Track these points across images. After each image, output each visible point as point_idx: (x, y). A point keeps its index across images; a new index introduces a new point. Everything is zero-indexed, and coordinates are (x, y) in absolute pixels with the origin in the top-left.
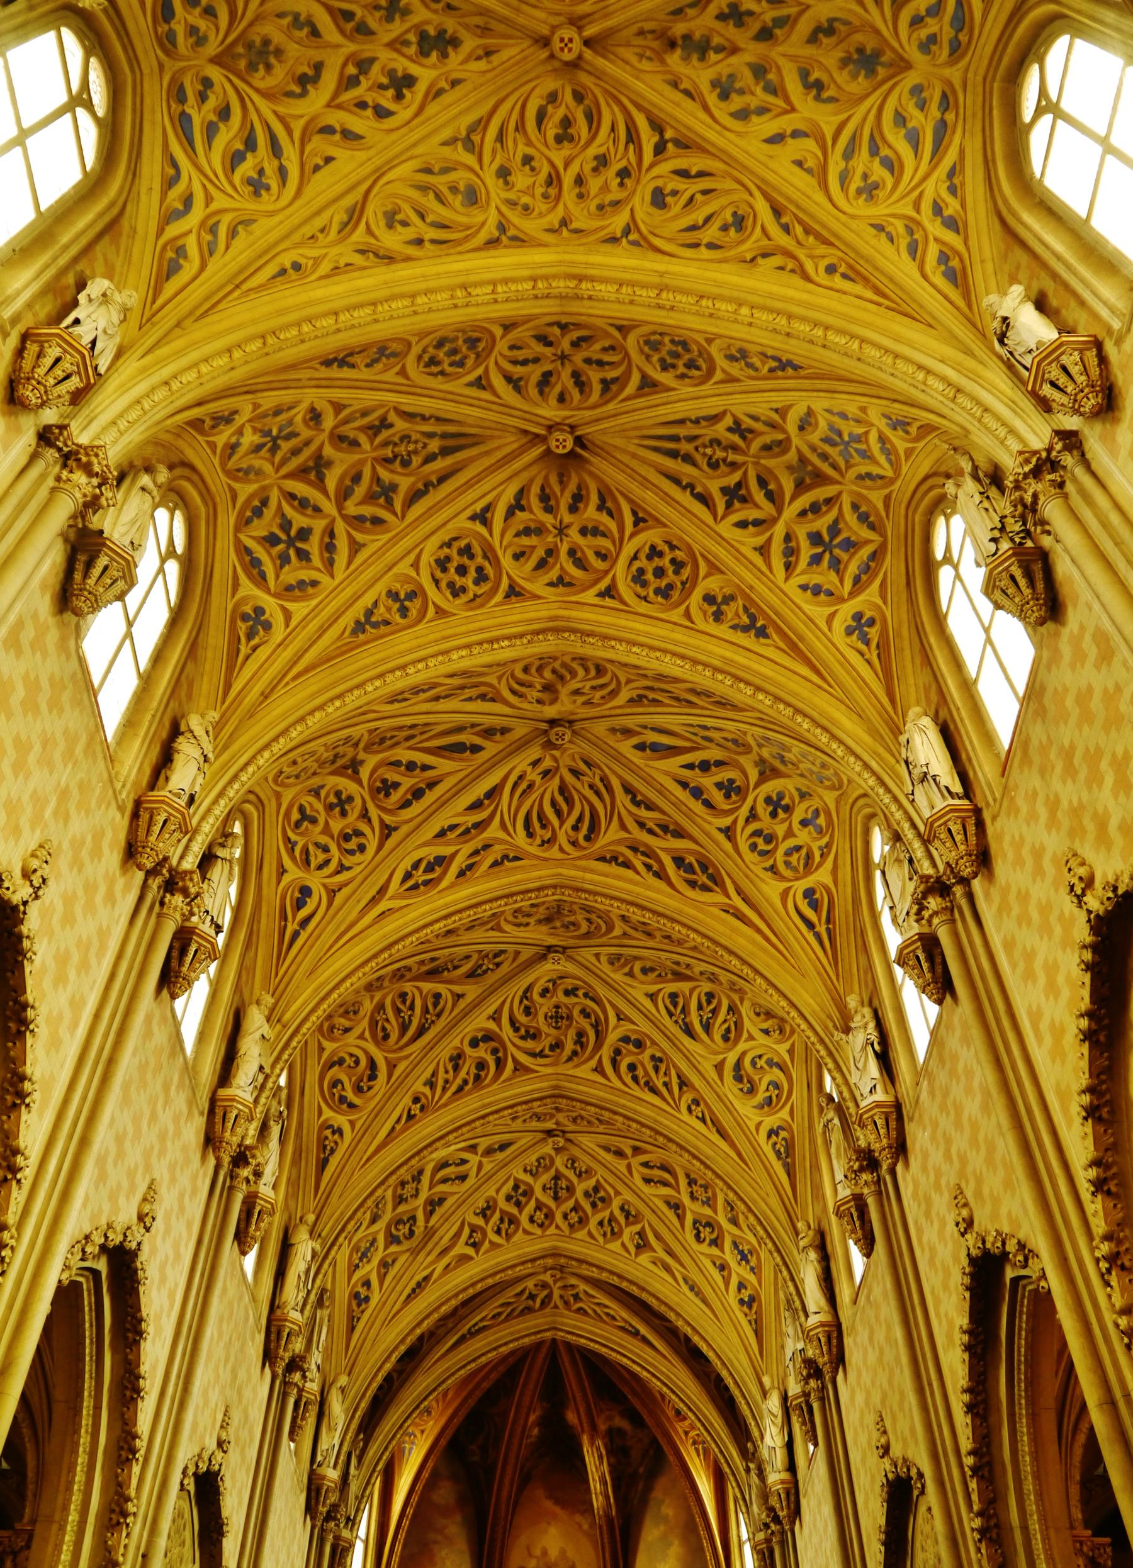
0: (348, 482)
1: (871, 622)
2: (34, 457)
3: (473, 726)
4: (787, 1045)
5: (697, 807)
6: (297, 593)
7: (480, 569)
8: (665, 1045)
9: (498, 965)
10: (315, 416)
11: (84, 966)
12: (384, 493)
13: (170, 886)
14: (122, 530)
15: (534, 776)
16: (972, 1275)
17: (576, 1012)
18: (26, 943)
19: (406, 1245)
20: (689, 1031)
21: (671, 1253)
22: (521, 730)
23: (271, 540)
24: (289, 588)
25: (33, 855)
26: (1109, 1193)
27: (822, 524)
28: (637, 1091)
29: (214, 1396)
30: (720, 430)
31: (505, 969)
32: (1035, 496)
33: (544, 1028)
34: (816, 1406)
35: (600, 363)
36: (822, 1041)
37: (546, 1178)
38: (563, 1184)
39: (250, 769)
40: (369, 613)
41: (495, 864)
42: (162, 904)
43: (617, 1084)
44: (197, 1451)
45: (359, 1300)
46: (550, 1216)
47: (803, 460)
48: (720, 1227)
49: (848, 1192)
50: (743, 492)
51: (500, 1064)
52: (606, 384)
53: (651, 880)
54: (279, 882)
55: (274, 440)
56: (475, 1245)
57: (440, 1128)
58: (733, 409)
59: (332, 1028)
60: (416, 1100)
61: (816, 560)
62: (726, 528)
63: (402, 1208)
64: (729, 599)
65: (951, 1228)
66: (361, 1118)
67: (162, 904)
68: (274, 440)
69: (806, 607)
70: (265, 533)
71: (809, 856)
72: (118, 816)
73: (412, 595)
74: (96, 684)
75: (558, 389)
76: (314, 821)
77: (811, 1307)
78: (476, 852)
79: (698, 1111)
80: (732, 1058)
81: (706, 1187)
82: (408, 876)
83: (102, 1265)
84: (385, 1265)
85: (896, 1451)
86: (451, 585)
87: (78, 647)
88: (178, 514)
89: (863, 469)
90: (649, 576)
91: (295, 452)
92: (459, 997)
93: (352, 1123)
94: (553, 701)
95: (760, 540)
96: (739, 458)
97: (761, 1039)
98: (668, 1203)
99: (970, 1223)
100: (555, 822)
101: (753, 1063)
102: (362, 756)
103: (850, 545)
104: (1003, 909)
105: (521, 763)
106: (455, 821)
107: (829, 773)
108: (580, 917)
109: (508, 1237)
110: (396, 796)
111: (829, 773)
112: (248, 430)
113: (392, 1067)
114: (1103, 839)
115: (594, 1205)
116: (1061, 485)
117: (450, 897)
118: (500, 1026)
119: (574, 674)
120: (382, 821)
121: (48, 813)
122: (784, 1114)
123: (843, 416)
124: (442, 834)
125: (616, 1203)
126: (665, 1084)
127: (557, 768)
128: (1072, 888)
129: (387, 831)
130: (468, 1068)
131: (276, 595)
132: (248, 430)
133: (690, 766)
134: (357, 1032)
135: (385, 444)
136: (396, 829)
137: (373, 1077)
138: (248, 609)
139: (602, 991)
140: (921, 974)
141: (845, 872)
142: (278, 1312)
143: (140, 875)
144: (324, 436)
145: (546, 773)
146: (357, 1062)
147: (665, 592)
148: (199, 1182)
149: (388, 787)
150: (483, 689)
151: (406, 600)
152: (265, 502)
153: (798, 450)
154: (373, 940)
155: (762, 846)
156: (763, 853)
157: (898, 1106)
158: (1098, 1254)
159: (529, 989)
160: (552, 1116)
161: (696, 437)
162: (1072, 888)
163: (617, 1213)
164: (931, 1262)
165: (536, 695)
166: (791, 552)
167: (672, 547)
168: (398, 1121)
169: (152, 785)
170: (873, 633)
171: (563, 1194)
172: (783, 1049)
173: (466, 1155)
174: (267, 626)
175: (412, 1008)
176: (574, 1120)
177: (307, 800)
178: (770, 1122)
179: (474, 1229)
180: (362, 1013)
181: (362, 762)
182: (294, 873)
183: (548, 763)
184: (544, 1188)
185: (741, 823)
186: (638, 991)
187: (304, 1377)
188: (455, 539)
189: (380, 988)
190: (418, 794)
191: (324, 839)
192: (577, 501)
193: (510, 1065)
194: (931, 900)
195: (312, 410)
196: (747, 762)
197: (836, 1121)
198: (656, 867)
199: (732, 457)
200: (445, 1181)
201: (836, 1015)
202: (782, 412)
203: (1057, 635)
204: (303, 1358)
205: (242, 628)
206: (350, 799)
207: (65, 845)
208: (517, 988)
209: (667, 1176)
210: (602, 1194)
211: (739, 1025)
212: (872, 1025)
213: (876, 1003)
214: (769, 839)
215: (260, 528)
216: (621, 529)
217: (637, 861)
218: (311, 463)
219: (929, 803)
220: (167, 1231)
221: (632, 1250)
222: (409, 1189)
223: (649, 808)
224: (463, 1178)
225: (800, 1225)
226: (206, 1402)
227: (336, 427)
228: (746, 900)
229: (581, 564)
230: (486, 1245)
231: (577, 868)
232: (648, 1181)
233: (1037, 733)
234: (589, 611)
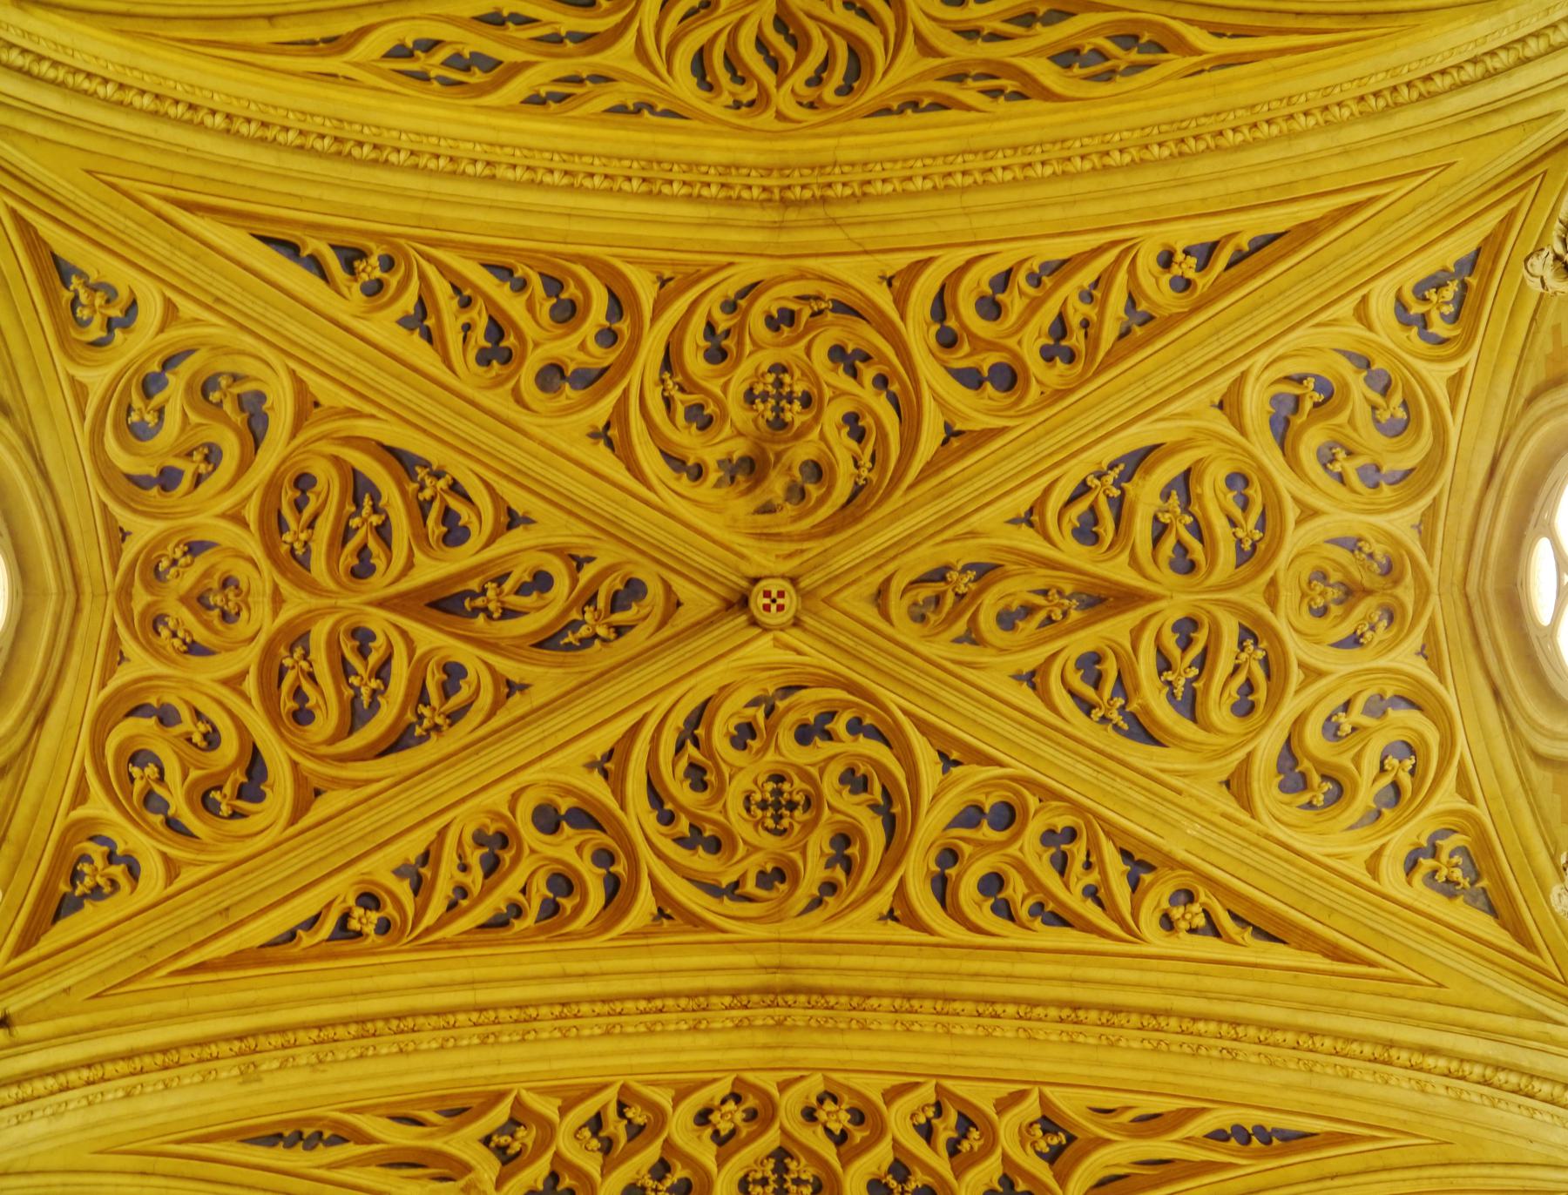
9: (620, 631)
17: (829, 785)
20: (1142, 731)
28: (1011, 935)
31: (637, 639)
33: (743, 828)
60: (369, 900)
80: (1268, 745)
82: (400, 52)
92: (513, 687)
100: (768, 77)
101: (1331, 730)
113: (308, 793)
118: (620, 795)
122: (1446, 798)
126: (1092, 893)
130: (523, 878)
134: (226, 665)
146: (212, 739)
159: (699, 716)
168: (312, 923)
175: (382, 672)
180: (243, 628)
186: (997, 670)
193: (645, 903)
198: (1010, 85)
217: (968, 94)
231: (818, 136)
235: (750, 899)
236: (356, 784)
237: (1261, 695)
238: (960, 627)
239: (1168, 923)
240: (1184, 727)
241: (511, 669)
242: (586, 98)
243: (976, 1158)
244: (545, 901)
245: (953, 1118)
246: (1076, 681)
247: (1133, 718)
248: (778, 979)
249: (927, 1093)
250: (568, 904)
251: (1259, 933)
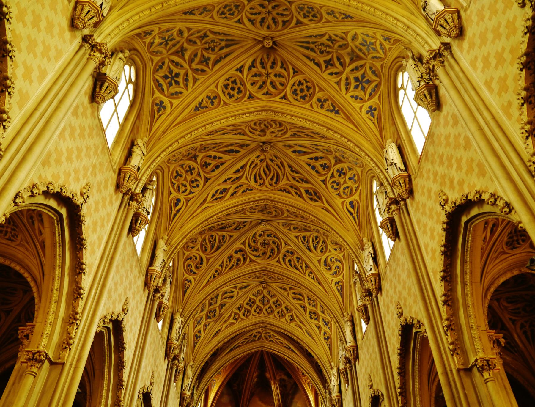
0: (193, 57)
1: (375, 109)
2: (81, 47)
3: (236, 143)
4: (342, 254)
5: (313, 173)
6: (175, 96)
7: (239, 89)
8: (301, 253)
9: (244, 226)
10: (181, 33)
11: (102, 226)
12: (205, 61)
13: (132, 199)
14: (113, 73)
15: (257, 161)
16: (402, 331)
17: (271, 242)
18: (82, 218)
19: (213, 319)
20: (309, 249)
21: (302, 322)
22: (253, 145)
23: (165, 77)
24: (172, 94)
25: (84, 188)
26: (448, 305)
27: (359, 74)
28: (291, 269)
29: (149, 368)
30: (324, 39)
31: (247, 227)
32: (434, 66)
34: (349, 372)
35: (282, 15)
36: (354, 253)
37: (260, 297)
38: (266, 299)
39: (159, 158)
40: (200, 104)
41: (244, 192)
42: (129, 205)
43: (285, 267)
44: (143, 386)
45: (197, 337)
46: (261, 310)
47: (353, 51)
48: (318, 314)
49: (361, 303)
50: (332, 62)
51: (245, 259)
52: (284, 22)
53: (297, 197)
54: (169, 197)
55: (167, 41)
56: (236, 319)
57: (224, 281)
58: (329, 32)
59: (187, 247)
60: (216, 271)
61: (356, 87)
62: (325, 75)
63: (211, 307)
64: (326, 100)
65: (395, 316)
66: (197, 277)
67: (129, 205)
68: (167, 41)
69: (353, 104)
70: (163, 75)
71: (351, 190)
72: (113, 174)
73: (215, 98)
74: (105, 128)
75: (267, 24)
76: (181, 176)
77: (348, 341)
78: (237, 188)
79: (312, 276)
80: (323, 258)
81: (314, 301)
82: (214, 195)
83: (110, 326)
84: (206, 326)
85: (375, 387)
86: (229, 94)
87: (98, 115)
88: (132, 67)
89: (374, 55)
90: (298, 92)
91: (174, 45)
92: (231, 237)
93: (195, 279)
94: (265, 135)
95: (337, 80)
96: (330, 50)
97: (334, 252)
98: (301, 306)
99: (402, 314)
101: (331, 260)
102: (198, 154)
103: (369, 82)
104: (417, 209)
105: (253, 157)
106: (230, 177)
107: (358, 162)
108: (273, 210)
109: (247, 317)
110: (210, 168)
111: (358, 162)
112: (157, 37)
113: (208, 260)
114: (452, 187)
115: (276, 306)
116: (443, 62)
117: (228, 203)
118: (245, 247)
119: (271, 126)
120: (205, 176)
121: (89, 173)
122: (341, 277)
123: (368, 35)
124: (225, 181)
126: (301, 267)
127: (266, 159)
128: (441, 203)
129: (207, 180)
130: (234, 261)
131: (167, 97)
132: (157, 37)
133: (311, 159)
134: (196, 248)
135: (206, 43)
136: (209, 179)
137: (202, 263)
138: (158, 102)
139: (280, 235)
140: (388, 231)
141: (364, 196)
142: (170, 341)
143: (121, 195)
144: (184, 40)
145: (261, 160)
146: (196, 258)
147: (304, 98)
148: (143, 298)
149: (207, 165)
150: (240, 131)
151: (213, 99)
152: (163, 63)
153: (351, 48)
154: (202, 217)
155: (335, 187)
156: (336, 189)
157: (379, 275)
158: (444, 325)
159: (255, 234)
160: (262, 277)
161: (315, 42)
162: (441, 203)
163: (284, 309)
164: (388, 327)
165: (258, 133)
166: (348, 84)
167: (307, 82)
169: (125, 164)
170: (376, 113)
172: (341, 255)
173: (233, 290)
174: (165, 108)
175: (215, 240)
176: (270, 278)
177: (179, 169)
178: (336, 279)
179: (235, 314)
180: (198, 242)
181: (198, 156)
182: (174, 194)
183: (262, 157)
184: (259, 301)
185: (328, 178)
186: (292, 235)
187: (179, 362)
188: (230, 78)
189: (204, 233)
190: (217, 167)
191: (185, 182)
192: (274, 64)
193: (248, 260)
194: (392, 206)
195: (180, 30)
196: (331, 157)
197: (358, 280)
198: (299, 193)
199: (328, 50)
200: (226, 298)
201: (359, 244)
202: (346, 34)
203: (439, 115)
204: (178, 356)
205: (156, 108)
206: (194, 169)
207: (95, 184)
208: (251, 234)
209: (301, 297)
210: (279, 303)
211: (326, 247)
212: (371, 248)
213: (373, 240)
214: (338, 184)
215: (162, 73)
216: (289, 75)
218: (179, 50)
219: (393, 173)
220: (132, 314)
221: (289, 321)
222: (214, 300)
223: (297, 173)
224: (232, 297)
225: (345, 314)
226: (146, 370)
227: (188, 37)
228: (330, 205)
229: (274, 87)
230: (240, 319)
231: (272, 193)
232: (294, 299)
233: (431, 149)
234: (277, 104)
236: (213, 257)
237: (324, 251)
238: (288, 228)
239: (309, 275)
240: (314, 251)
241: (230, 234)
242: (240, 190)
246: (302, 239)
247: (308, 247)
251: (318, 283)
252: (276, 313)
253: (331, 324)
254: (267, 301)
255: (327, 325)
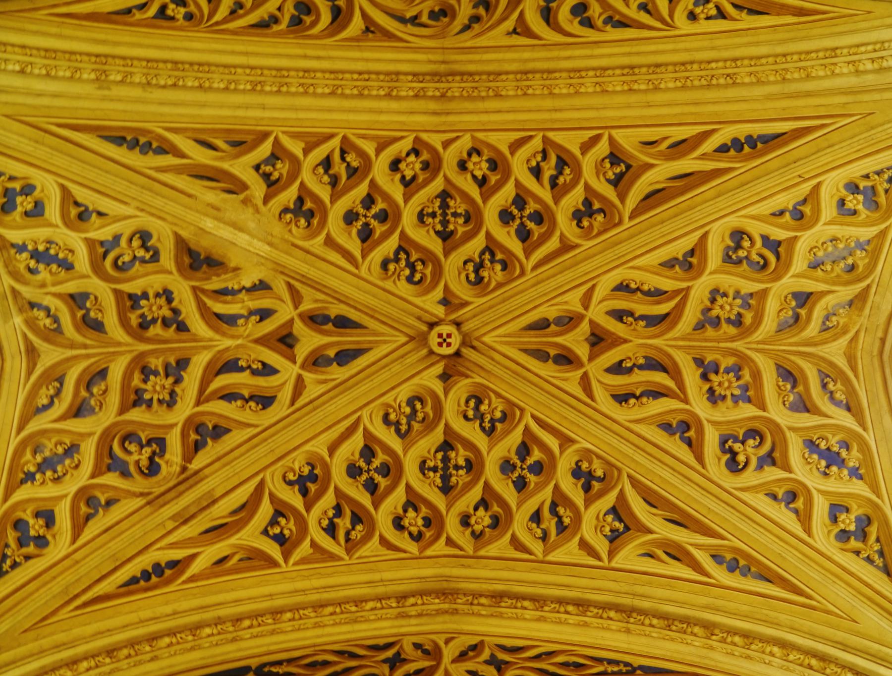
19: (139, 484)
38: (460, 456)
48: (776, 429)
56: (280, 539)
63: (137, 415)
84: (89, 504)
109: (351, 545)
125: (565, 463)
171: (459, 478)
179: (280, 511)
193: (357, 24)
200: (229, 396)
209: (660, 378)
221: (601, 546)
224: (265, 401)
230: (305, 549)
232: (622, 398)
235: (425, 26)
243: (568, 188)
244: (293, 16)
245: (553, 160)
248: (442, 68)
249: (537, 143)
250: (308, 20)
252: (520, 525)
253: (864, 448)
254: (469, 465)
255: (842, 463)
